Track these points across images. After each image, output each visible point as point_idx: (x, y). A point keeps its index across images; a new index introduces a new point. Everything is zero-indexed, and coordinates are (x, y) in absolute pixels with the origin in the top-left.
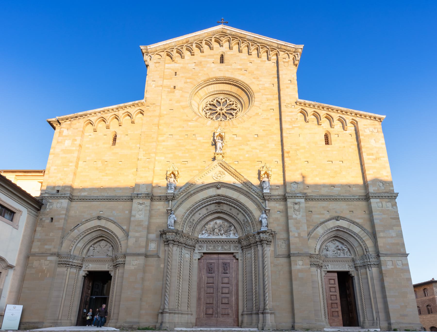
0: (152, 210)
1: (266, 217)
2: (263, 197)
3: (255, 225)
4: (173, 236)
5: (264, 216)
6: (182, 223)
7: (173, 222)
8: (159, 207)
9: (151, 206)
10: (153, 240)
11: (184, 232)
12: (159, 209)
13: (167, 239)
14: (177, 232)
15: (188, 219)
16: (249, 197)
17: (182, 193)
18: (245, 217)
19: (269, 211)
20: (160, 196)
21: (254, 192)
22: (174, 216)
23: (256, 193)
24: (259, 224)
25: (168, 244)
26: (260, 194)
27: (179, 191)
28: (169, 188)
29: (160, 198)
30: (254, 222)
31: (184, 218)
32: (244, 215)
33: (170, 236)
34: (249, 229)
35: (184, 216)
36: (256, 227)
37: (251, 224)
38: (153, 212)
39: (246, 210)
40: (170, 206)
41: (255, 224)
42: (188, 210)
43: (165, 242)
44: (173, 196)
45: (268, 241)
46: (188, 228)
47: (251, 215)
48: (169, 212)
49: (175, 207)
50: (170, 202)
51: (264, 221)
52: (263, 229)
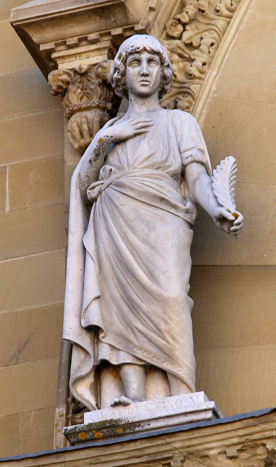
7: (172, 276)
22: (179, 131)
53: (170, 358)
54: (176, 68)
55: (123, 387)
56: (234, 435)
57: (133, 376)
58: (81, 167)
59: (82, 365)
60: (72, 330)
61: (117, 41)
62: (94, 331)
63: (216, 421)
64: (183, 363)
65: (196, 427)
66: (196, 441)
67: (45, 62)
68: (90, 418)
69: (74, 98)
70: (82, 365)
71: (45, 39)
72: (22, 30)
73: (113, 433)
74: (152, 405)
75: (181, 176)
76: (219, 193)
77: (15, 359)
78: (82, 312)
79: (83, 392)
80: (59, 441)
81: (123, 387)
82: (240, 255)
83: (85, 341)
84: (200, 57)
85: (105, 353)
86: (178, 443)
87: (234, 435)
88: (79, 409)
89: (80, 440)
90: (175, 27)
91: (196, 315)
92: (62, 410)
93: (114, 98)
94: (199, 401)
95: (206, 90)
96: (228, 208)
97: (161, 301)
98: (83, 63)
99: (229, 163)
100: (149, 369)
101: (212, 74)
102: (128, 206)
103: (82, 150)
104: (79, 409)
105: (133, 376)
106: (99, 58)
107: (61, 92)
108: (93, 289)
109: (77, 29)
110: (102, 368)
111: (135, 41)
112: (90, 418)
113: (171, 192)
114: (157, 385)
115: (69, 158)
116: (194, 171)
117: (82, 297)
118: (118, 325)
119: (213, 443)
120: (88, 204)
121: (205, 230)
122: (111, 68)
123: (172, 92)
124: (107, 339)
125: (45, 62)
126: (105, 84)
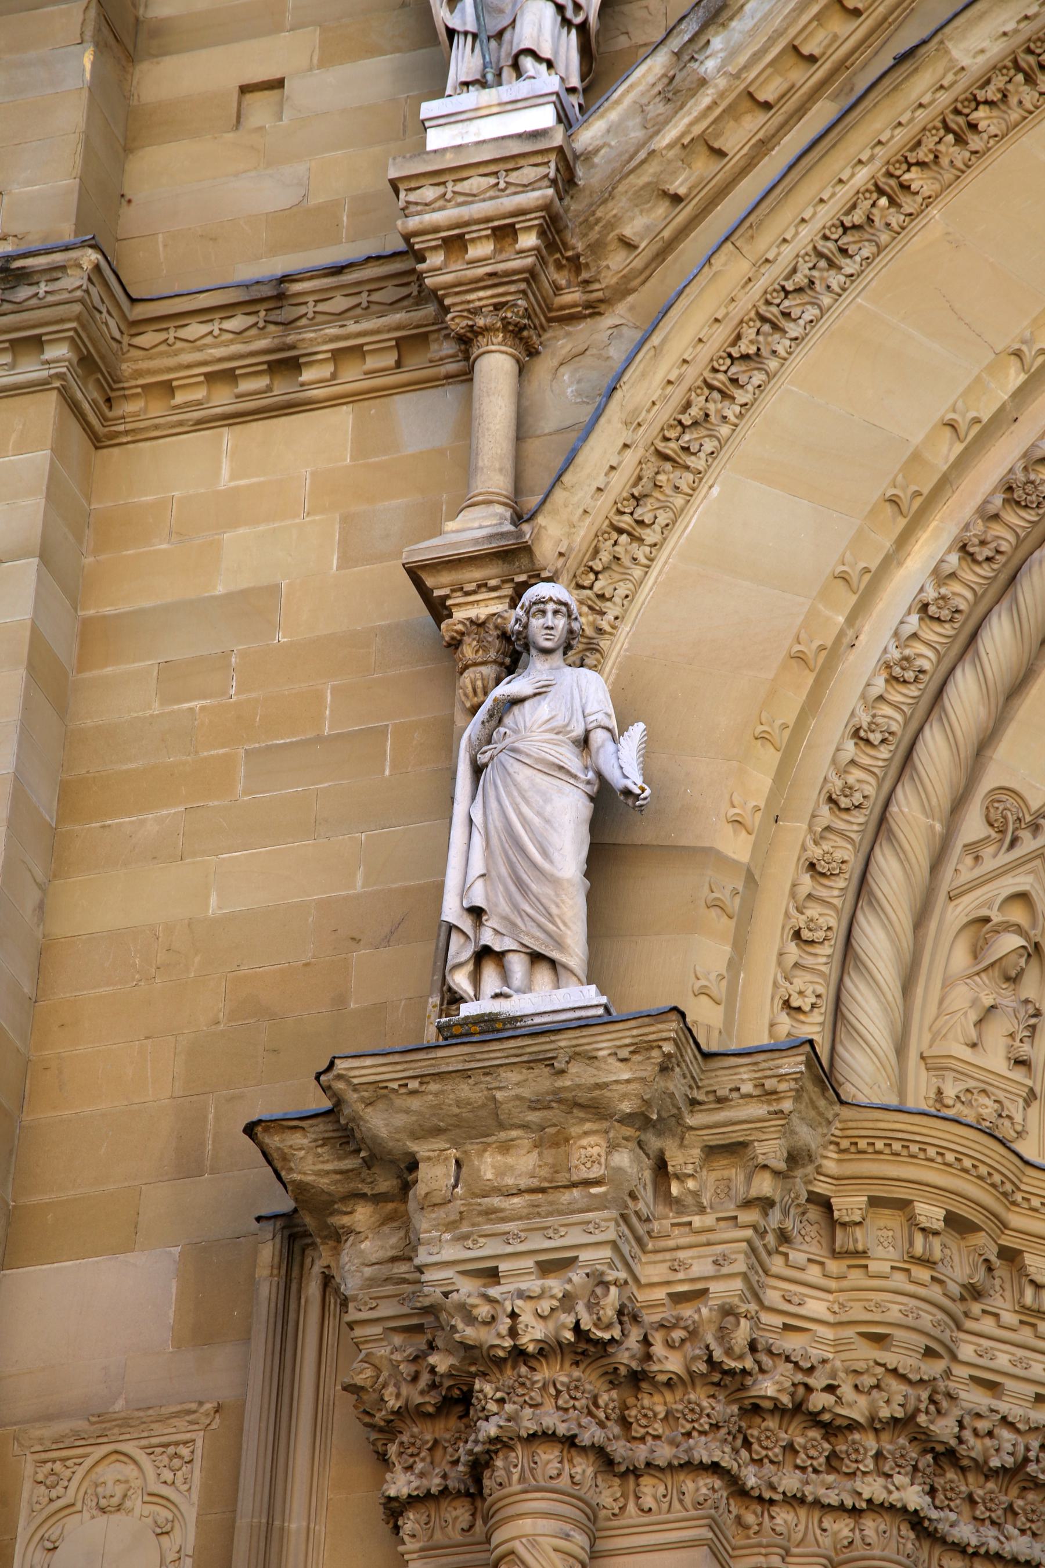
0: (95, 638)
4: (590, 1238)
6: (784, 872)
8: (242, 559)
9: (72, 545)
10: (103, 1426)
11: (865, 1072)
12: (257, 604)
13: (426, 1323)
14: (672, 1095)
15: (936, 754)
17: (752, 125)
20: (274, 297)
25: (474, 1486)
27: (674, 92)
28: (464, 62)
29: (276, 338)
31: (830, 734)
33: (507, 1246)
35: (822, 664)
38: (127, 695)
40: (493, 476)
42: (911, 512)
43: (384, 1433)
44: (552, 226)
46: (955, 990)
48: (471, 628)
49: (606, 464)
50: (496, 365)
53: (560, 945)
54: (585, 621)
55: (505, 976)
56: (627, 1035)
57: (517, 965)
58: (473, 728)
59: (460, 951)
60: (452, 911)
61: (521, 589)
62: (476, 913)
63: (608, 1018)
64: (575, 952)
65: (584, 1025)
66: (583, 1040)
67: (439, 609)
68: (466, 1010)
69: (468, 651)
70: (460, 951)
71: (439, 584)
72: (414, 573)
73: (491, 1027)
74: (537, 998)
75: (584, 743)
76: (625, 763)
77: (388, 940)
78: (464, 890)
79: (461, 981)
80: (430, 1035)
81: (505, 976)
82: (644, 833)
83: (466, 924)
84: (612, 610)
85: (487, 938)
86: (563, 1041)
87: (627, 1035)
88: (455, 999)
89: (453, 1034)
90: (586, 574)
91: (592, 899)
92: (436, 999)
93: (514, 653)
94: (590, 995)
95: (617, 648)
96: (634, 780)
97: (553, 881)
98: (480, 612)
99: (637, 731)
100: (536, 958)
101: (625, 629)
102: (522, 774)
103: (474, 710)
104: (455, 999)
105: (517, 965)
106: (499, 607)
107: (455, 644)
108: (478, 865)
109: (476, 574)
110: (484, 954)
111: (541, 590)
112: (466, 1010)
113: (571, 760)
114: (543, 976)
115: (459, 718)
116: (599, 737)
117: (465, 874)
118: (504, 907)
119: (603, 1043)
120: (477, 770)
121: (607, 804)
122: (512, 620)
123: (578, 648)
124: (491, 922)
125: (439, 609)
126: (505, 636)
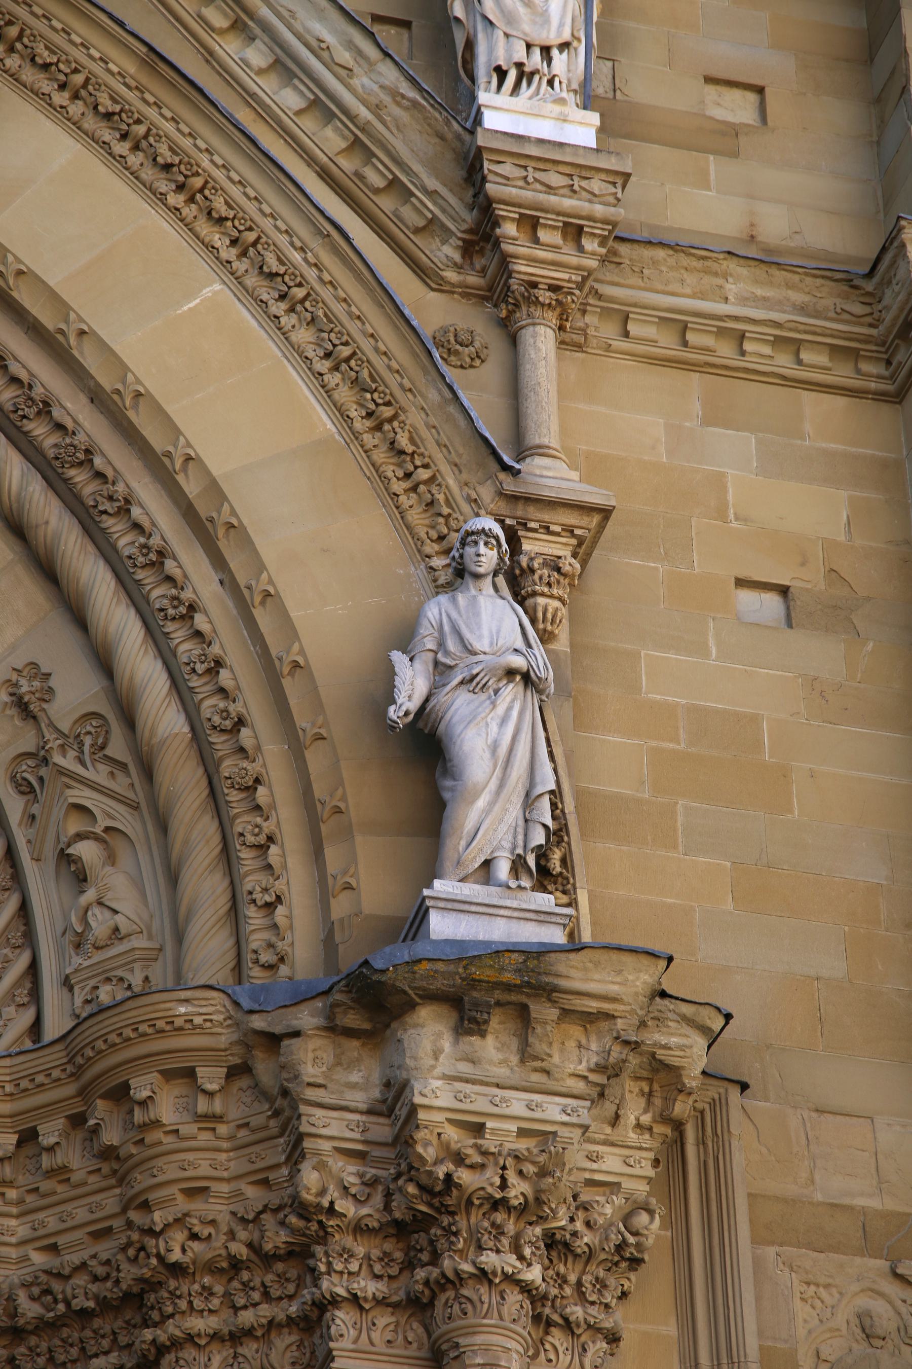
1: (539, 660)
2: (482, 238)
3: (287, 820)
5: (492, 622)
16: (179, 185)
18: (77, 615)
19: (584, 550)
21: (290, 99)
23: (330, 141)
24: (364, 789)
26: (412, 145)
30: (273, 761)
32: (47, 570)
34: (123, 893)
36: (290, 852)
37: (182, 780)
39: (113, 453)
41: (278, 791)
45: (556, 1246)
47: (203, 583)
51: (489, 737)
52: (470, 916)
